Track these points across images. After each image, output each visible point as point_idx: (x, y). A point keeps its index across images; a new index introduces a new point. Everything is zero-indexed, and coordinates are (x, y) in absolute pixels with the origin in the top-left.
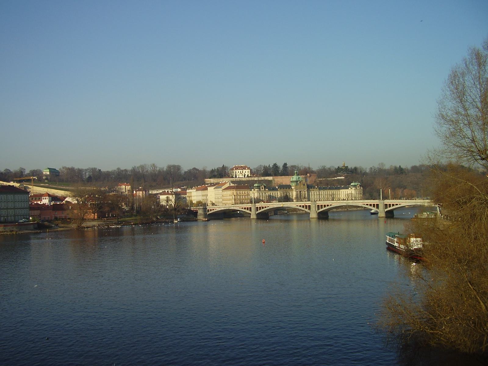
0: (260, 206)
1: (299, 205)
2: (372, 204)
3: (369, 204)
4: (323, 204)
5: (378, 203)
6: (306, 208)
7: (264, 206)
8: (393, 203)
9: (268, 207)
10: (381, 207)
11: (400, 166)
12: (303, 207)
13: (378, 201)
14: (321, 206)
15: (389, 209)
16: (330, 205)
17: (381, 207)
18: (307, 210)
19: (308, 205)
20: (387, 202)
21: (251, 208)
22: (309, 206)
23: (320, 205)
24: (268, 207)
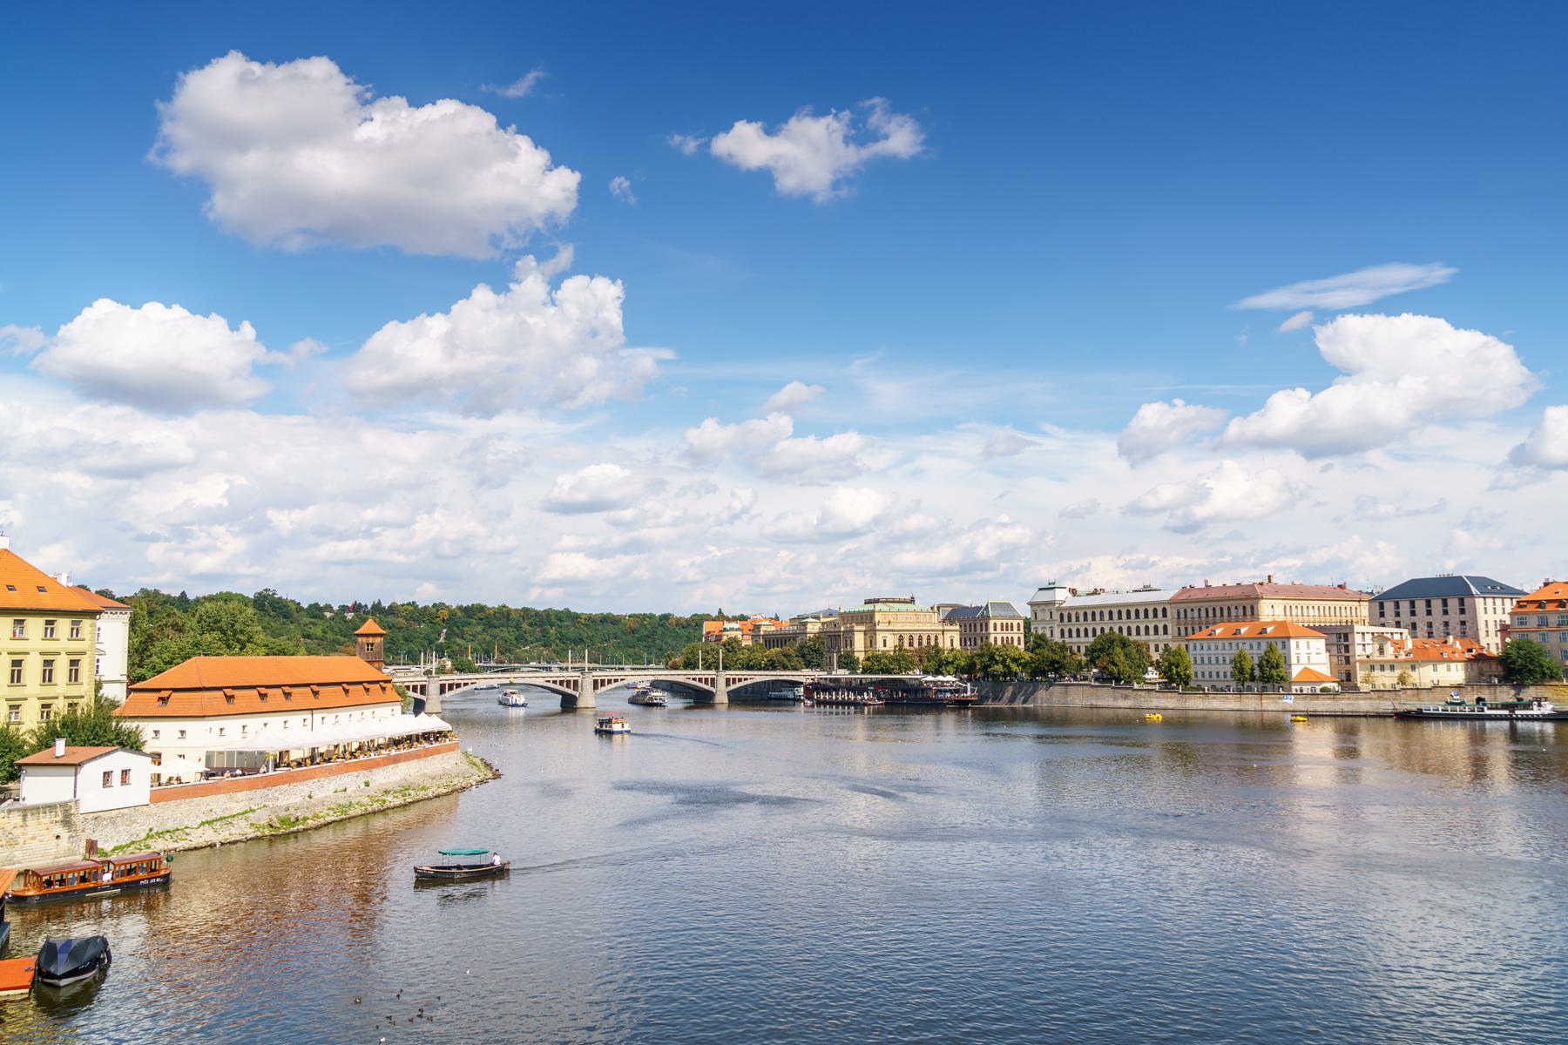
0: (609, 678)
1: (551, 679)
2: (703, 677)
3: (697, 677)
4: (606, 678)
5: (714, 676)
6: (567, 687)
7: (462, 682)
8: (740, 677)
9: (472, 683)
10: (721, 682)
11: (183, 594)
12: (561, 683)
13: (713, 672)
14: (603, 681)
15: (733, 687)
16: (622, 680)
17: (721, 682)
18: (570, 691)
19: (572, 679)
20: (732, 674)
21: (423, 688)
22: (576, 682)
23: (599, 679)
24: (472, 683)
